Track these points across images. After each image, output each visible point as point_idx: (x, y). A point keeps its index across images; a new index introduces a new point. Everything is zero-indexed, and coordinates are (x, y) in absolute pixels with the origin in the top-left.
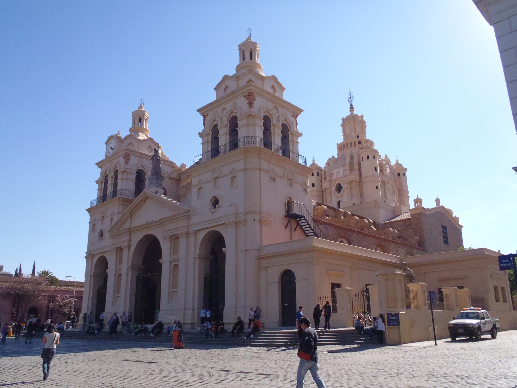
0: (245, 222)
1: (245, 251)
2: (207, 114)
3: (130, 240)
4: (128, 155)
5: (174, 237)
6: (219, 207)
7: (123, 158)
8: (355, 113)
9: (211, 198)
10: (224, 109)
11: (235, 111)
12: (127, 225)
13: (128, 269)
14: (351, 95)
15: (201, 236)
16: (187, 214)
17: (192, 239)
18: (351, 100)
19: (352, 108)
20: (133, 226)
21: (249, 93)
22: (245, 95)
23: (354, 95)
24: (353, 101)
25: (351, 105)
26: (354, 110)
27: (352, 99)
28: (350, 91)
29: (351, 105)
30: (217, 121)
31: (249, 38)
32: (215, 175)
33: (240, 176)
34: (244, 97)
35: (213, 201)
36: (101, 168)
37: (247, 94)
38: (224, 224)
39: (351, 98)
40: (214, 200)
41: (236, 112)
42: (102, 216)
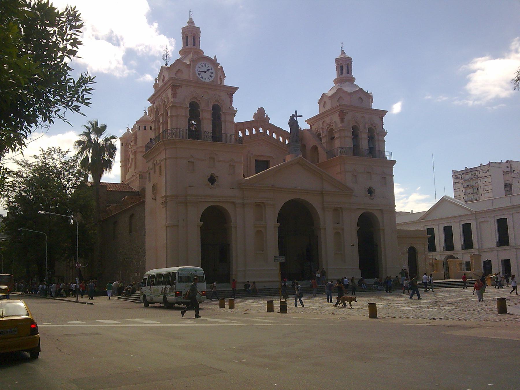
11: (375, 125)
14: (168, 54)
15: (359, 214)
18: (166, 59)
28: (166, 49)
39: (166, 57)
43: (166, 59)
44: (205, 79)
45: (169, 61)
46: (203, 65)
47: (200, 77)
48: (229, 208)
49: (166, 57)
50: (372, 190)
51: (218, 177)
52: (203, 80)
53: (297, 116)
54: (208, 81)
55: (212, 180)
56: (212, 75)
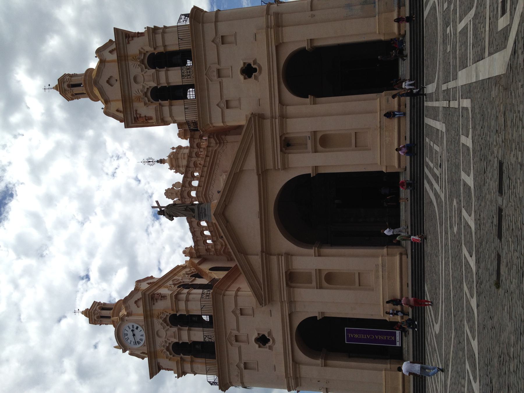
0: (277, 15)
1: (312, 10)
2: (135, 112)
3: (279, 255)
4: (154, 294)
5: (284, 149)
6: (255, 62)
7: (156, 304)
8: (166, 158)
9: (242, 77)
10: (135, 79)
12: (256, 261)
13: (319, 255)
14: (146, 161)
16: (257, 117)
17: (290, 110)
18: (152, 162)
19: (162, 161)
20: (259, 249)
21: (126, 37)
22: (127, 41)
23: (147, 158)
24: (154, 159)
25: (158, 162)
26: (164, 159)
27: (151, 161)
29: (158, 162)
30: (148, 89)
31: (56, 88)
32: (215, 74)
33: (224, 28)
34: (129, 43)
35: (246, 76)
36: (159, 369)
37: (127, 40)
38: (277, 47)
39: (150, 162)
40: (245, 75)
41: (145, 54)
42: (234, 342)
43: (152, 162)
44: (142, 335)
45: (154, 159)
46: (126, 337)
47: (142, 343)
48: (298, 321)
49: (150, 162)
50: (246, 66)
51: (259, 334)
52: (144, 338)
53: (159, 206)
54: (143, 333)
55: (263, 340)
56: (135, 327)
